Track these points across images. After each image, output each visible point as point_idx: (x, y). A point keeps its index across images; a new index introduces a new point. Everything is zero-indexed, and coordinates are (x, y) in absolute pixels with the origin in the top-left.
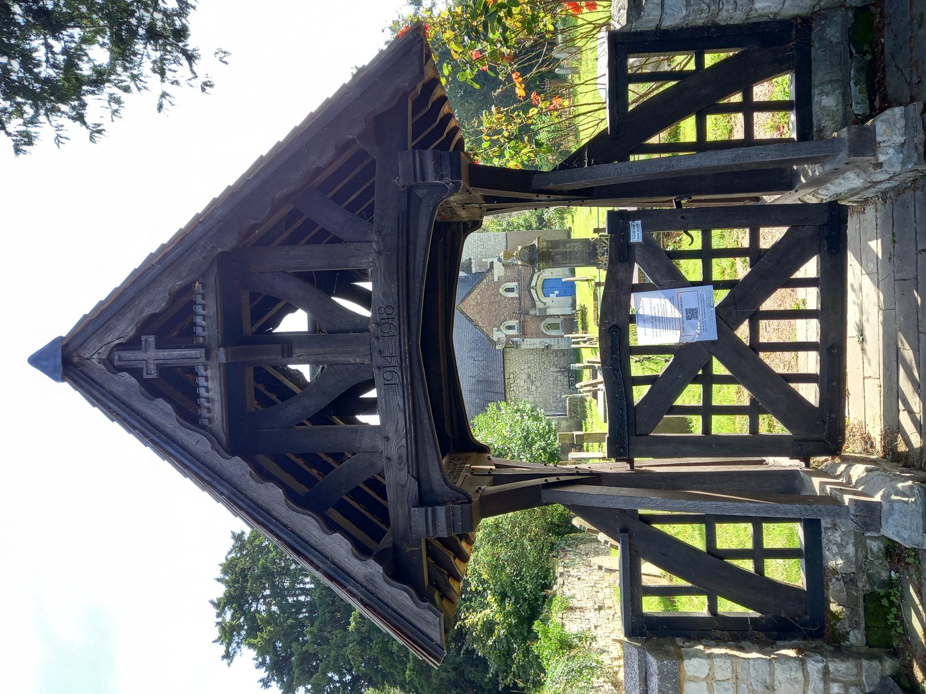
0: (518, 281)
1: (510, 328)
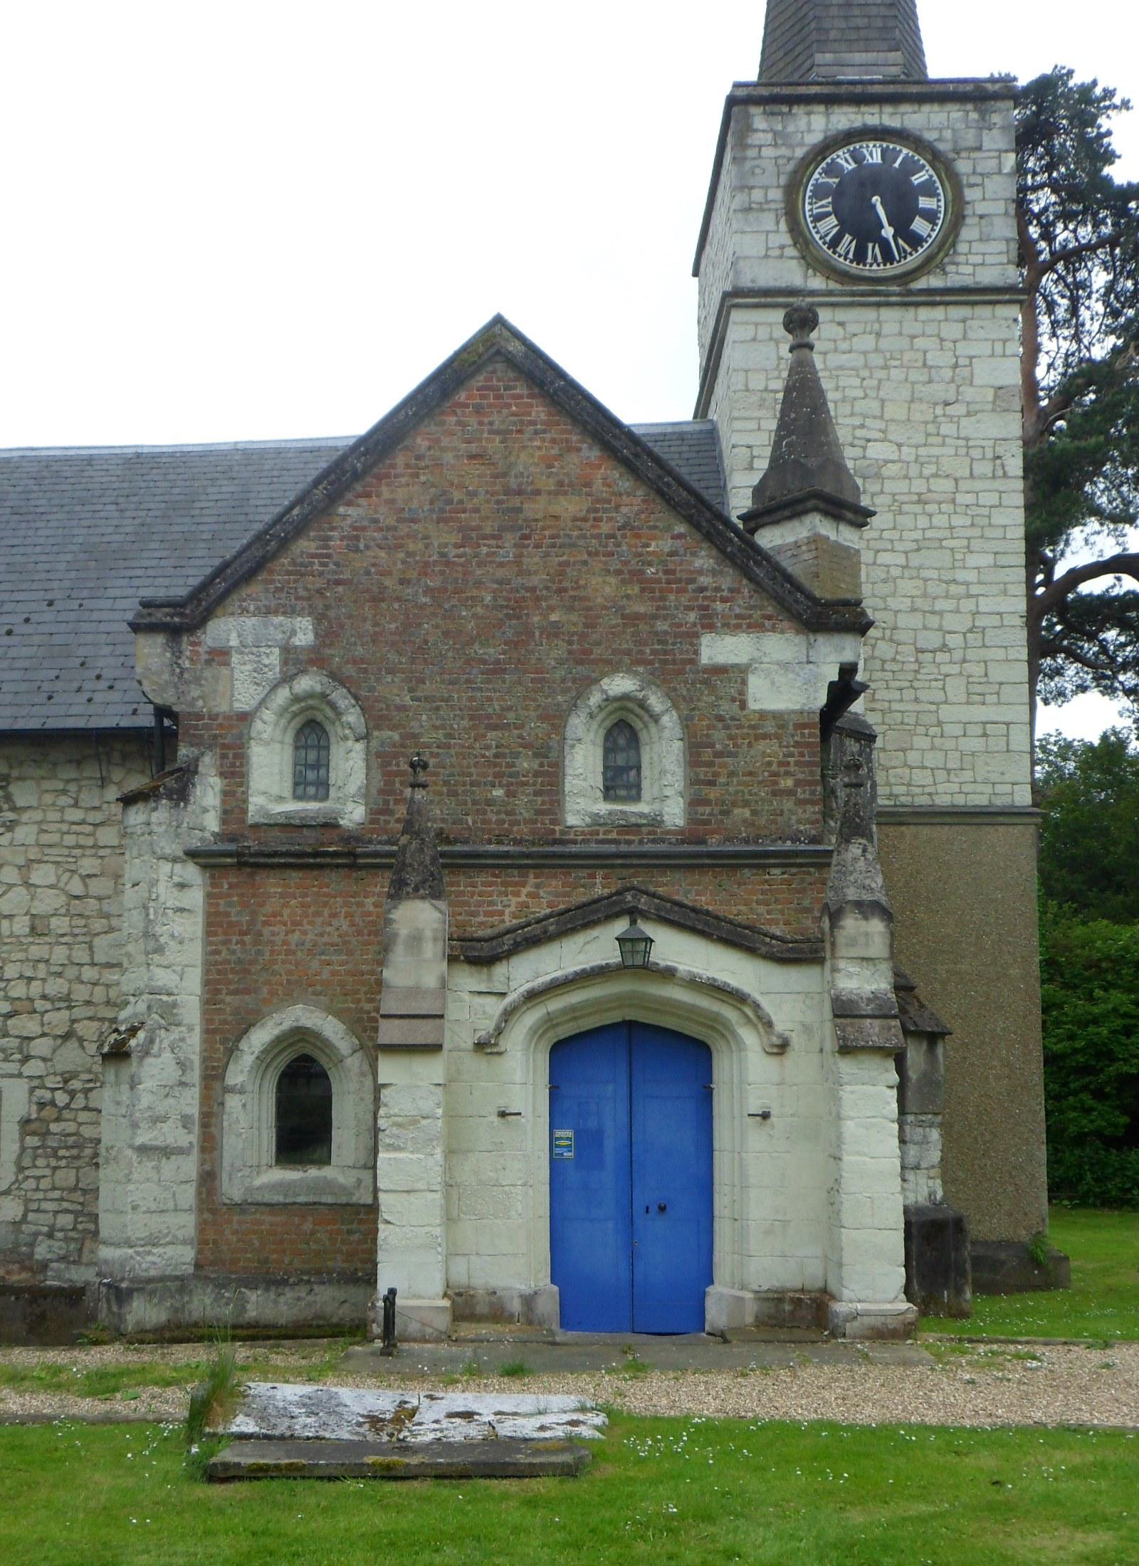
0: (695, 832)
1: (311, 774)
